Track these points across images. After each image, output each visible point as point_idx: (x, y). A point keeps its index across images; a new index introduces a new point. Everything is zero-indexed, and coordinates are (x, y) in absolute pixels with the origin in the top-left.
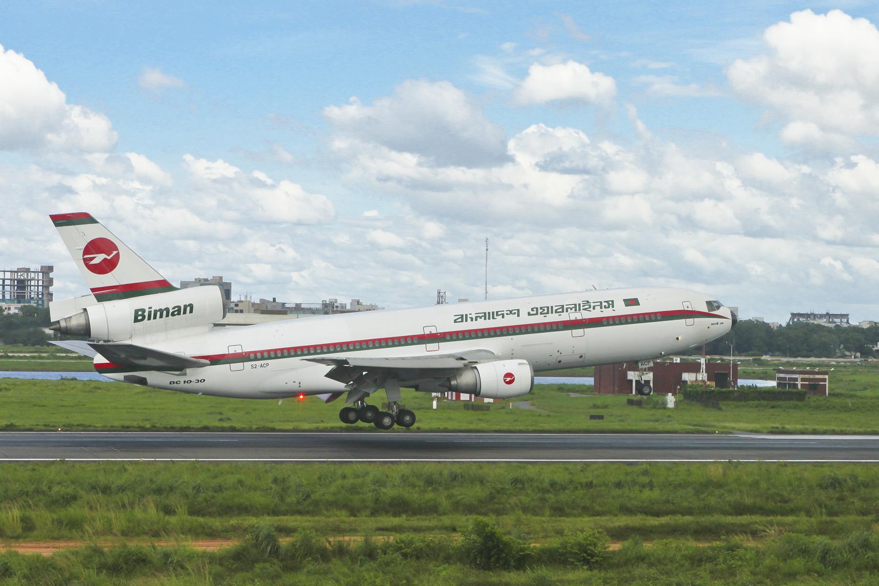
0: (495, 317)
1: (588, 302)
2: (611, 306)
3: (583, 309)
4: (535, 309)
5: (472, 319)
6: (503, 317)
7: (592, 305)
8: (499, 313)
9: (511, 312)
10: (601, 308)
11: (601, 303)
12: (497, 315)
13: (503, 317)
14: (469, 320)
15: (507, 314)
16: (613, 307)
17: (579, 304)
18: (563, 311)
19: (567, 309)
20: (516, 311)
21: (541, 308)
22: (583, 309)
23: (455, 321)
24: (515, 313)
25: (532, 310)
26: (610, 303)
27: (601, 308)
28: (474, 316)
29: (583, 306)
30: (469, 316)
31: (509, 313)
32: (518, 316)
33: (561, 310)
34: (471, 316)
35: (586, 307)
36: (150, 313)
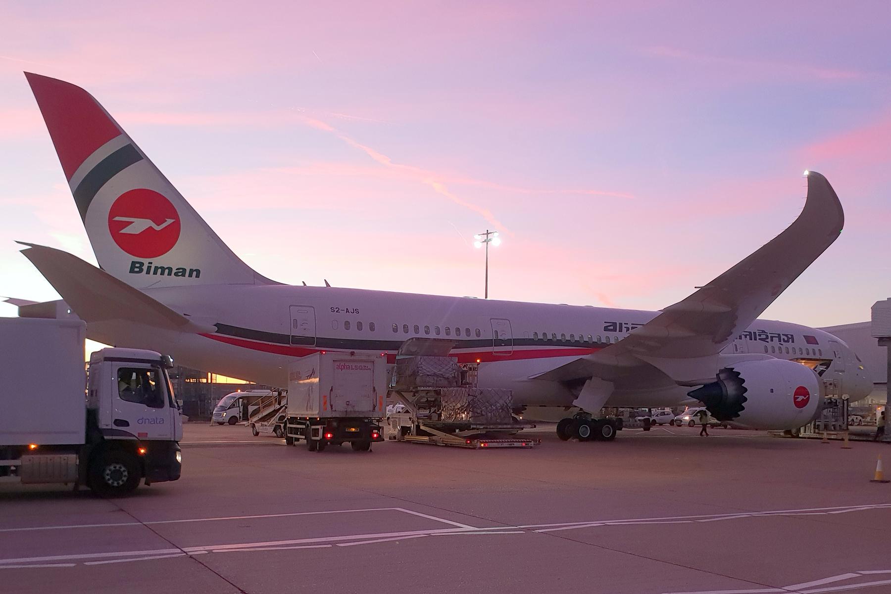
1: (763, 331)
3: (759, 339)
22: (759, 339)
27: (780, 341)
30: (624, 326)
34: (626, 326)
36: (149, 268)
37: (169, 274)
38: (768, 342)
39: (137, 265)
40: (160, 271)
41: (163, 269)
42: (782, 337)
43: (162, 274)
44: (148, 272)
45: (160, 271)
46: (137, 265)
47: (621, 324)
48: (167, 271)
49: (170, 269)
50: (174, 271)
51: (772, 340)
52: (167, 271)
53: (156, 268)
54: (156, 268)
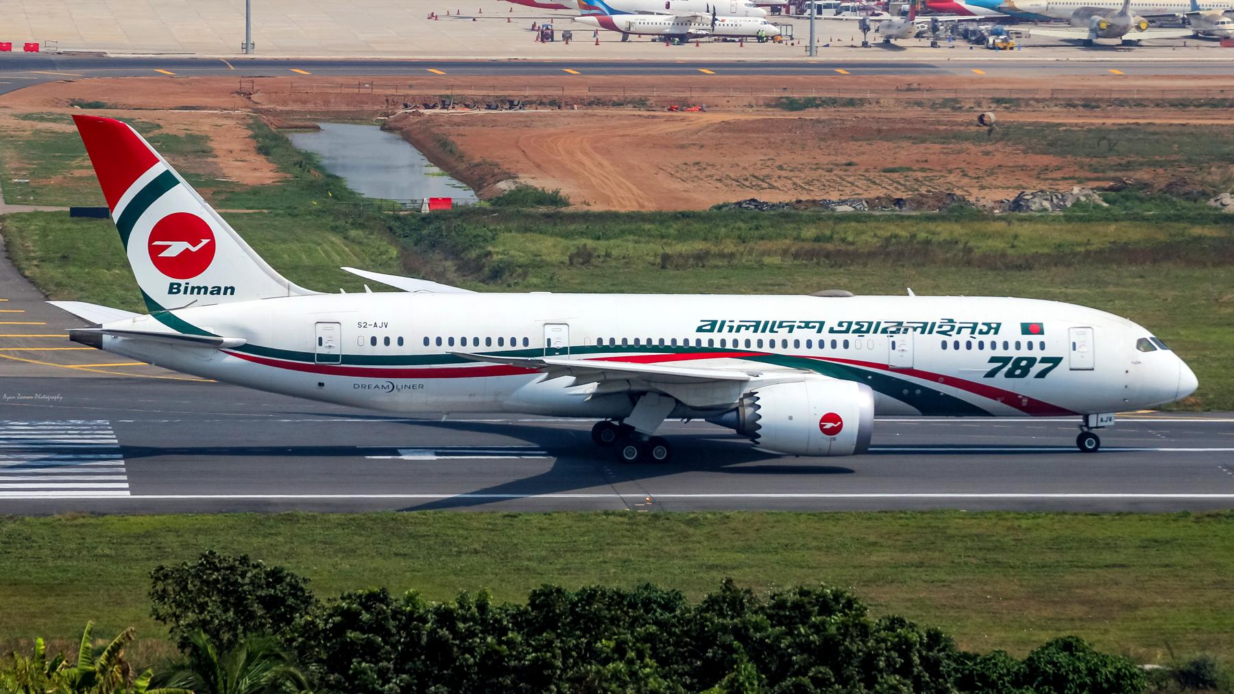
0: (775, 329)
1: (951, 321)
2: (993, 331)
3: (938, 332)
4: (845, 325)
5: (730, 331)
6: (791, 331)
7: (957, 326)
8: (784, 324)
9: (807, 325)
10: (973, 332)
11: (976, 325)
12: (780, 326)
13: (791, 331)
14: (726, 329)
15: (799, 327)
16: (996, 333)
17: (934, 324)
18: (898, 331)
19: (906, 330)
20: (817, 325)
21: (858, 323)
22: (938, 332)
23: (700, 330)
24: (814, 327)
25: (840, 324)
26: (994, 326)
27: (973, 332)
28: (735, 325)
29: (940, 327)
30: (727, 323)
31: (803, 325)
32: (819, 331)
33: (894, 329)
34: (731, 324)
35: (945, 328)
36: (186, 288)
37: (205, 293)
38: (950, 335)
39: (175, 286)
40: (196, 290)
41: (199, 288)
42: (980, 327)
43: (199, 293)
44: (185, 293)
45: (196, 290)
46: (175, 286)
47: (723, 323)
48: (203, 290)
49: (206, 288)
50: (210, 290)
51: (959, 332)
52: (203, 290)
53: (193, 288)
54: (193, 288)
